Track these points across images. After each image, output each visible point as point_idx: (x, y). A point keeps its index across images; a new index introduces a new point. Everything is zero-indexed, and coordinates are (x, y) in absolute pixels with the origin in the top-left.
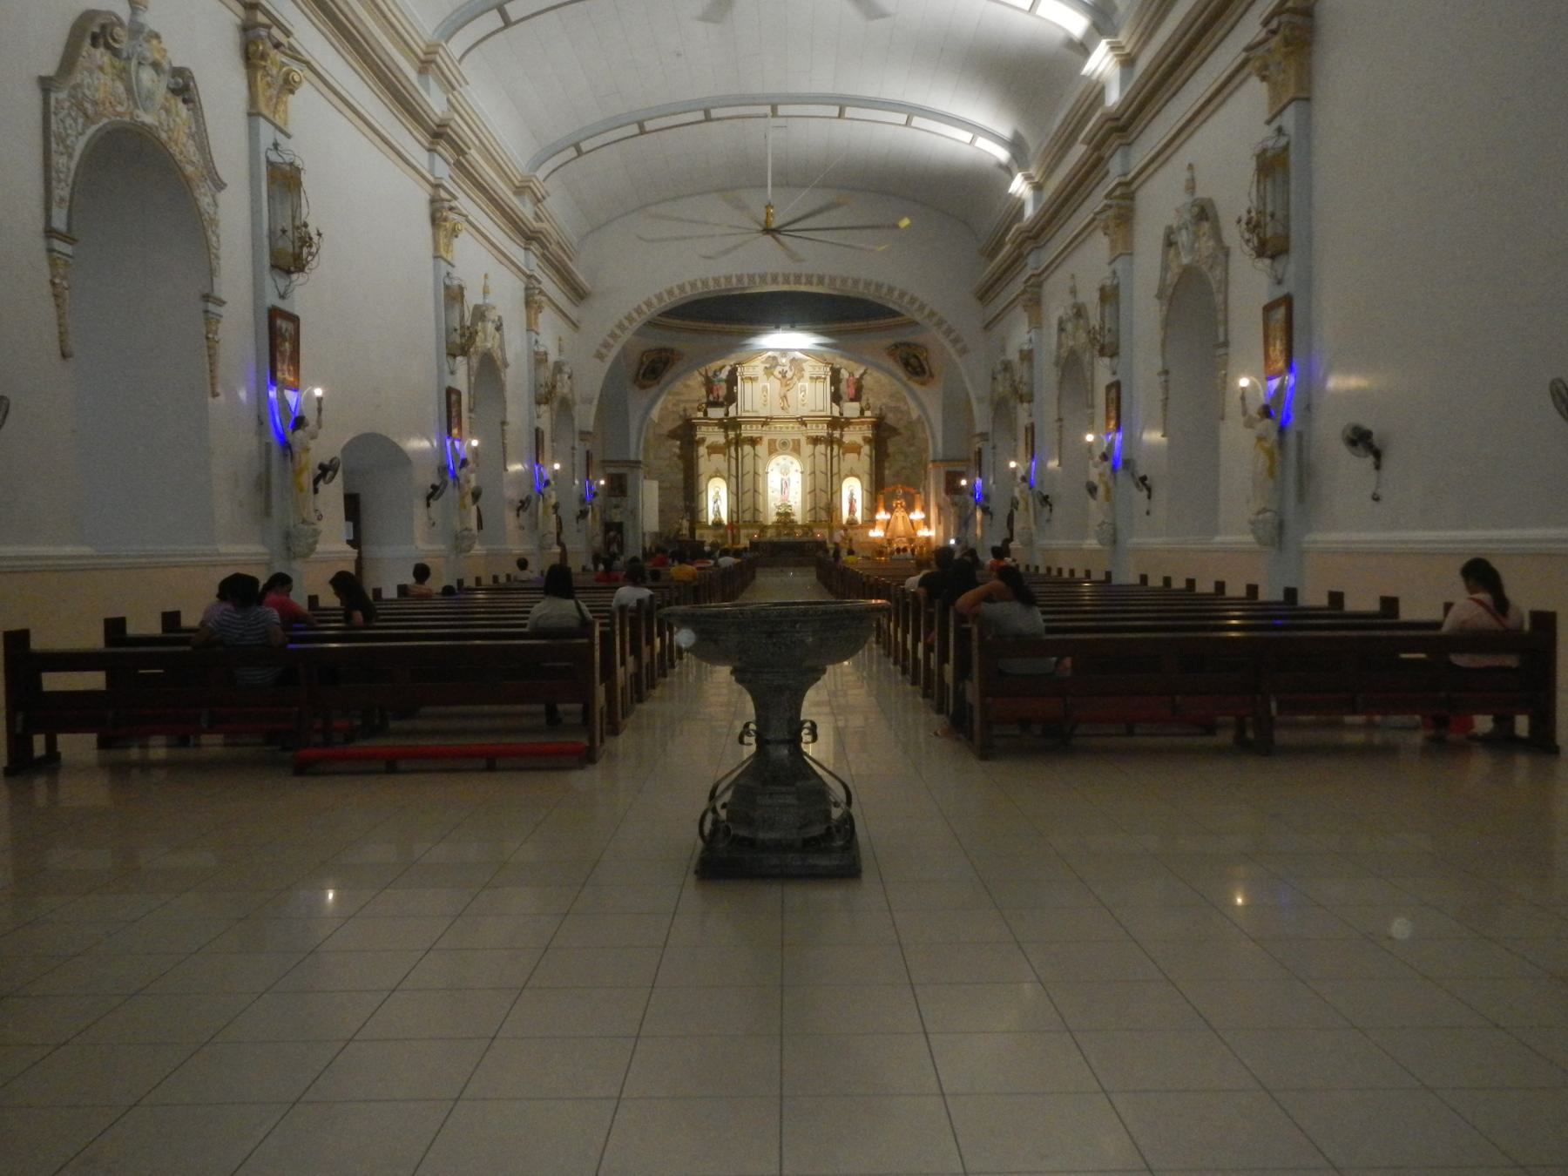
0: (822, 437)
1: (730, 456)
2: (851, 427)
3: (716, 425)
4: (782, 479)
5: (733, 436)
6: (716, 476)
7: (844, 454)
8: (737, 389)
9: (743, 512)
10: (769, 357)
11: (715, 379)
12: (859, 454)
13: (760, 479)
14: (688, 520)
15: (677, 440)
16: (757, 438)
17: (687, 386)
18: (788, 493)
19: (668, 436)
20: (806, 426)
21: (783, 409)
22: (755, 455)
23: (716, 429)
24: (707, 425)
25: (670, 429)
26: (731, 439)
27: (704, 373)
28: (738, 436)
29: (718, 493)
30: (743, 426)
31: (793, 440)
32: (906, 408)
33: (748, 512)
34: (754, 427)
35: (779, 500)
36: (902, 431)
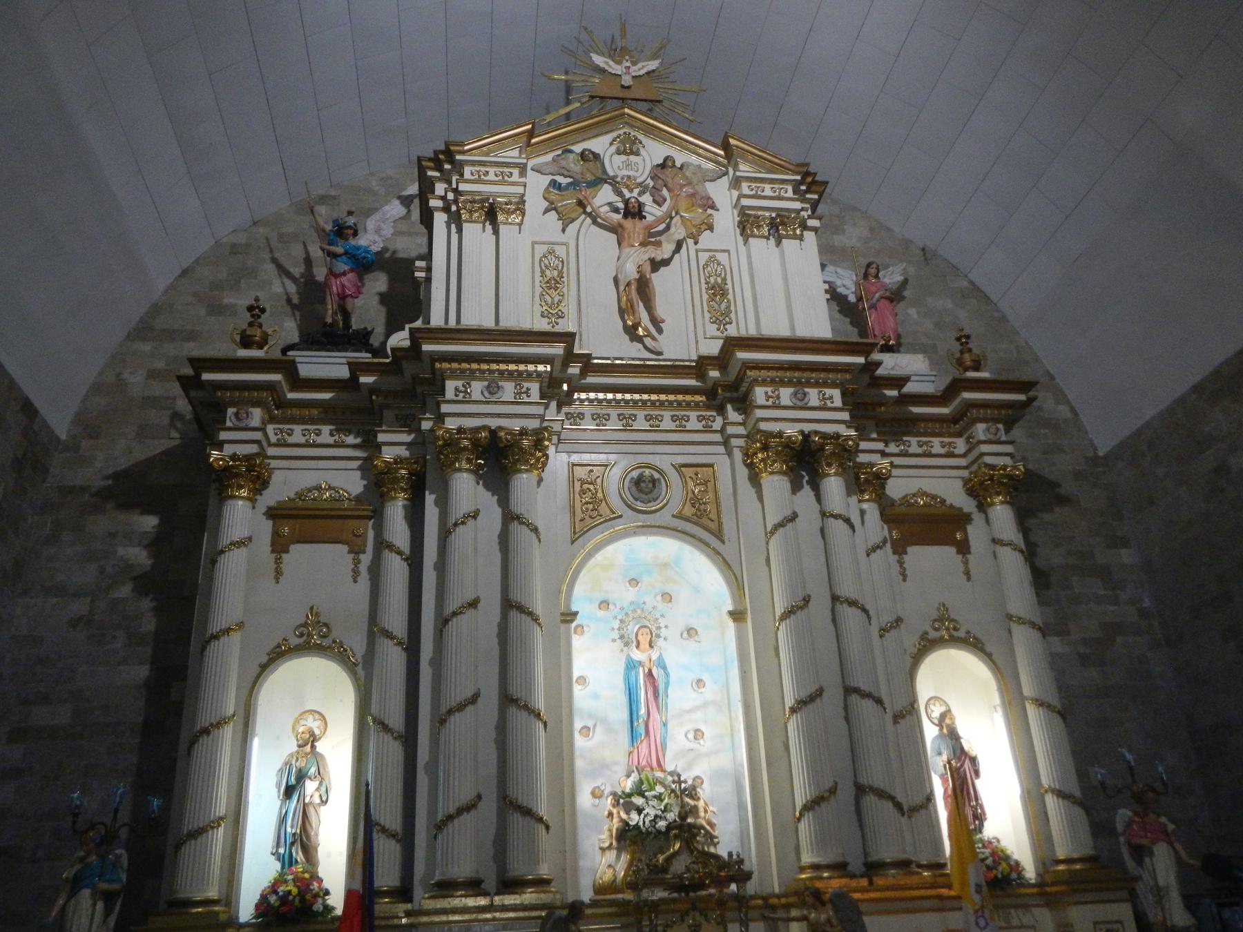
0: (837, 436)
1: (382, 545)
2: (914, 444)
3: (327, 414)
4: (631, 666)
5: (403, 452)
6: (306, 647)
7: (900, 549)
8: (429, 269)
9: (439, 827)
10: (571, 151)
11: (339, 250)
12: (963, 548)
13: (539, 639)
14: (109, 897)
15: (146, 511)
16: (523, 432)
17: (217, 309)
18: (665, 725)
19: (105, 494)
20: (744, 404)
21: (631, 332)
22: (510, 517)
23: (326, 433)
24: (281, 411)
25: (124, 463)
26: (398, 461)
27: (297, 271)
28: (421, 442)
29: (312, 739)
30: (451, 386)
31: (679, 468)
32: (1063, 411)
33: (465, 817)
34: (508, 390)
35: (621, 770)
36: (1069, 487)
